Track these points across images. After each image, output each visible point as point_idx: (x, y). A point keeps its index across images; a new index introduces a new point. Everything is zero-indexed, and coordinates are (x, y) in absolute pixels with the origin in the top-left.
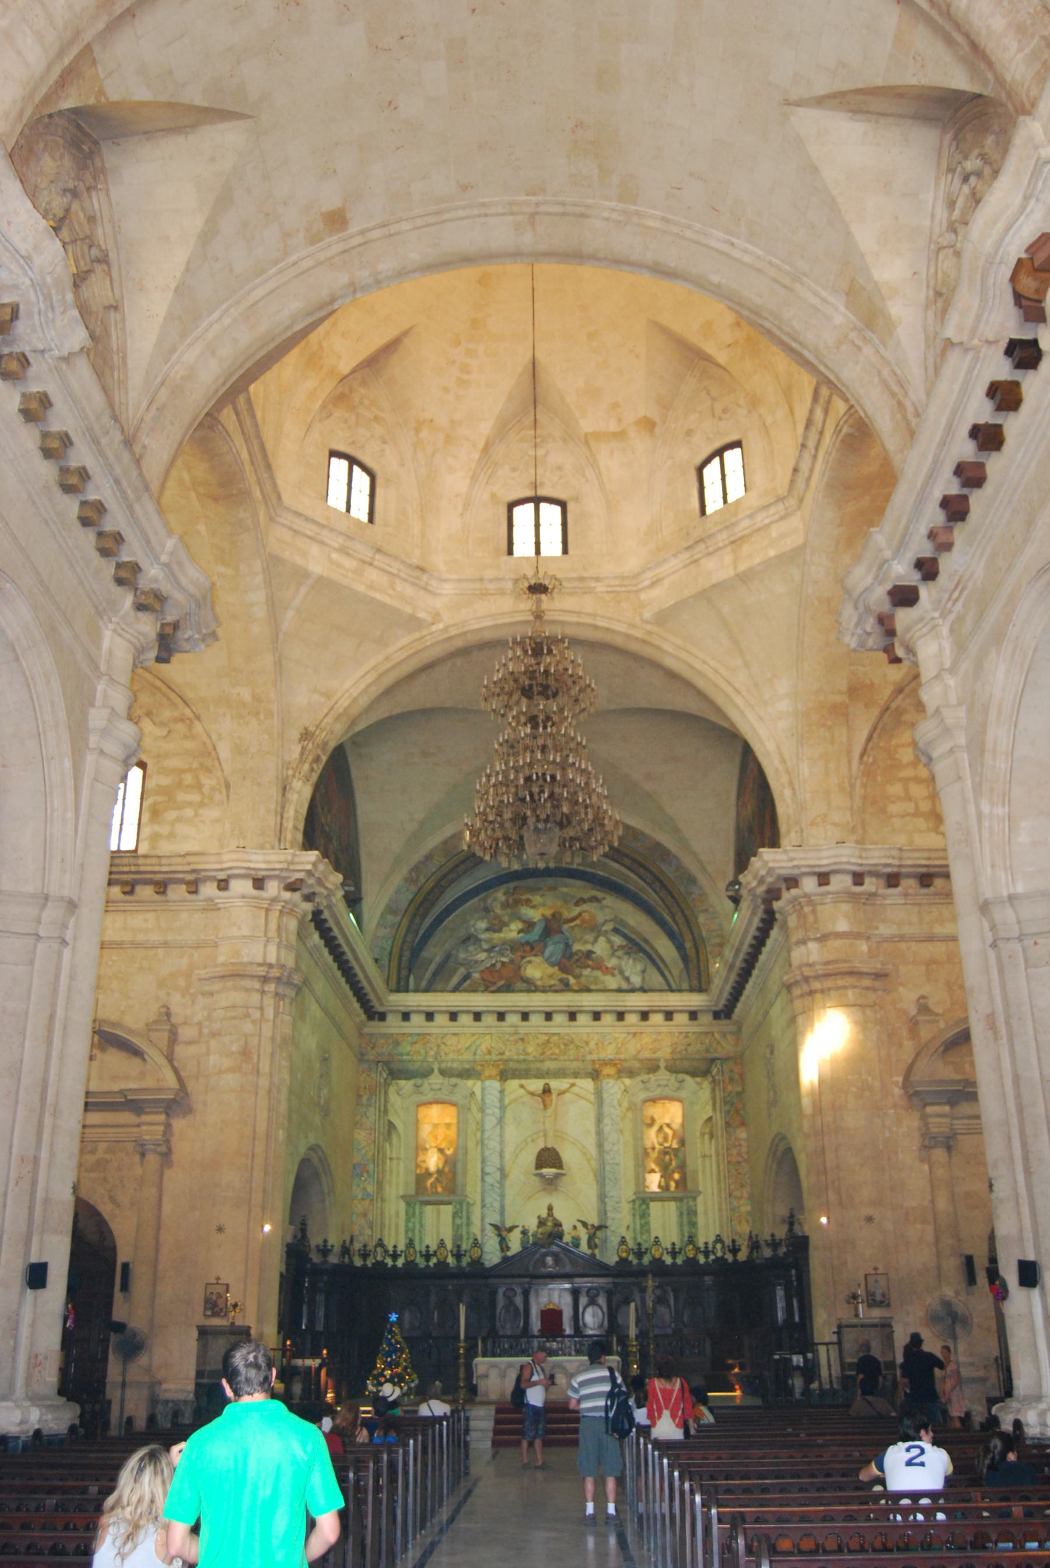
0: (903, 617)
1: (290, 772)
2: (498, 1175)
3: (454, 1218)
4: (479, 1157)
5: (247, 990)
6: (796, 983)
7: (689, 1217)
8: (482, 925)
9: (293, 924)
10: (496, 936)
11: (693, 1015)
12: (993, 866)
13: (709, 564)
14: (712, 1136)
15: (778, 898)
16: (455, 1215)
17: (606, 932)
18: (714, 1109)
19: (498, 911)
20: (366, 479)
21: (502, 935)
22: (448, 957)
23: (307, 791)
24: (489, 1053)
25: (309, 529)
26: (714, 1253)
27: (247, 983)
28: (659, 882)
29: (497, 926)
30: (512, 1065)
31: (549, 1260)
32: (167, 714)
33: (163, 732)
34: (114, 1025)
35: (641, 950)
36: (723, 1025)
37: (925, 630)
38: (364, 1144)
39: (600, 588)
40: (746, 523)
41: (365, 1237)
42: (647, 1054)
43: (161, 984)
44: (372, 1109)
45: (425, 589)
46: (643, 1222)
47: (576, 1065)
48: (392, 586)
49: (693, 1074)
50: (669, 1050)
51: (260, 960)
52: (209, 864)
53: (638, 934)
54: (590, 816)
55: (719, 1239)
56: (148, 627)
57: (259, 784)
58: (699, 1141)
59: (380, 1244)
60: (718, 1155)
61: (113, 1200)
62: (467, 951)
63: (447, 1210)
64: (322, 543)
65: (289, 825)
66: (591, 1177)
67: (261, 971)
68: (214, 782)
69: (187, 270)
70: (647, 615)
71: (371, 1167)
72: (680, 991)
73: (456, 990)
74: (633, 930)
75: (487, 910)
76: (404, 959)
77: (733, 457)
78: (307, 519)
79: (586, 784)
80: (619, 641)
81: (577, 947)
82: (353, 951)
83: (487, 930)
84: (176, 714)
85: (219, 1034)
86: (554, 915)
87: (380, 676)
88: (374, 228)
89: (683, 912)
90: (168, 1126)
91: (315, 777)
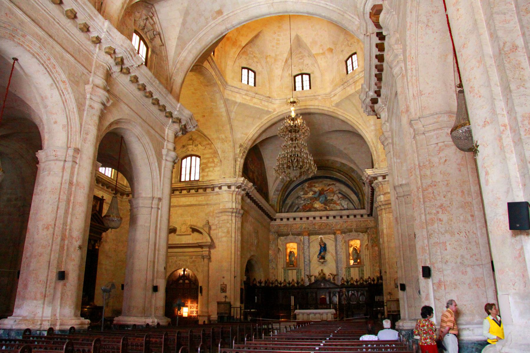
0: (376, 106)
1: (237, 156)
2: (308, 262)
5: (227, 215)
6: (378, 207)
7: (362, 272)
8: (302, 193)
9: (240, 197)
10: (306, 196)
11: (362, 216)
12: (397, 176)
13: (348, 89)
14: (368, 250)
15: (373, 183)
16: (297, 272)
17: (337, 193)
19: (306, 189)
20: (253, 74)
21: (308, 196)
22: (293, 203)
23: (242, 161)
24: (305, 228)
25: (236, 90)
26: (368, 281)
27: (228, 214)
28: (351, 179)
29: (306, 193)
30: (311, 231)
31: (322, 285)
32: (205, 143)
33: (203, 148)
34: (194, 226)
35: (347, 198)
36: (371, 218)
37: (382, 110)
39: (320, 98)
40: (357, 76)
41: (272, 278)
42: (349, 227)
43: (206, 215)
44: (274, 245)
45: (271, 103)
47: (329, 231)
48: (261, 103)
49: (362, 233)
50: (355, 226)
51: (231, 207)
52: (216, 183)
53: (346, 193)
54: (308, 166)
55: (369, 278)
56: (177, 127)
57: (229, 160)
58: (364, 251)
59: (277, 280)
60: (369, 254)
61: (197, 270)
62: (298, 201)
64: (240, 93)
65: (237, 170)
66: (334, 261)
67: (231, 210)
68: (218, 160)
69: (180, 33)
70: (333, 105)
71: (274, 260)
72: (358, 209)
73: (295, 212)
74: (344, 193)
75: (303, 189)
76: (281, 204)
77: (355, 57)
78: (235, 88)
79: (307, 157)
80: (326, 113)
81: (328, 198)
82: (261, 203)
83: (303, 194)
84: (207, 143)
85: (221, 227)
86: (322, 189)
87: (260, 128)
88: (230, 13)
89: (358, 186)
90: (210, 251)
91: (244, 157)
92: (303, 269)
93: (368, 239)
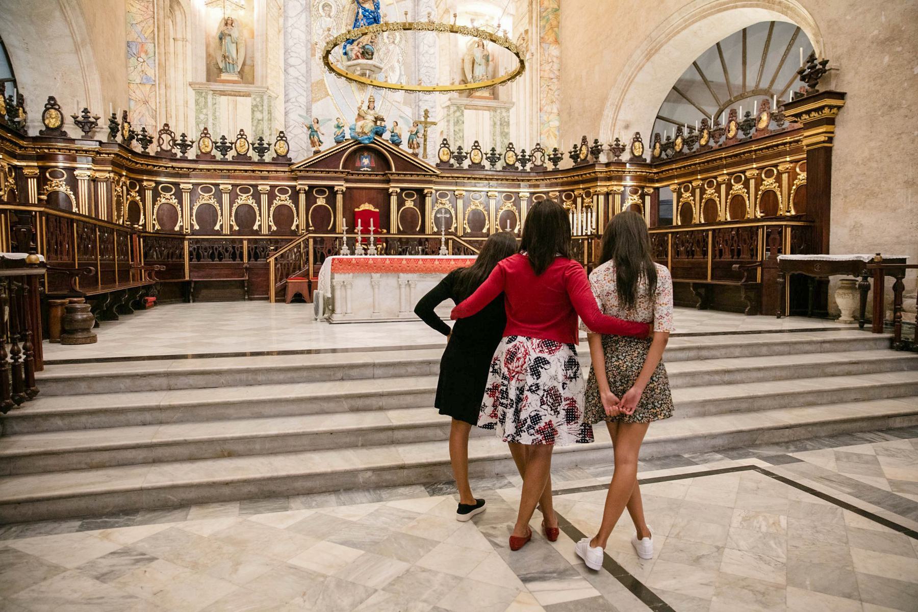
3: (253, 112)
4: (281, 45)
18: (530, 23)
38: (140, 18)
46: (457, 128)
55: (538, 148)
59: (166, 129)
63: (246, 103)
71: (150, 47)
92: (282, 97)
93: (531, 11)
